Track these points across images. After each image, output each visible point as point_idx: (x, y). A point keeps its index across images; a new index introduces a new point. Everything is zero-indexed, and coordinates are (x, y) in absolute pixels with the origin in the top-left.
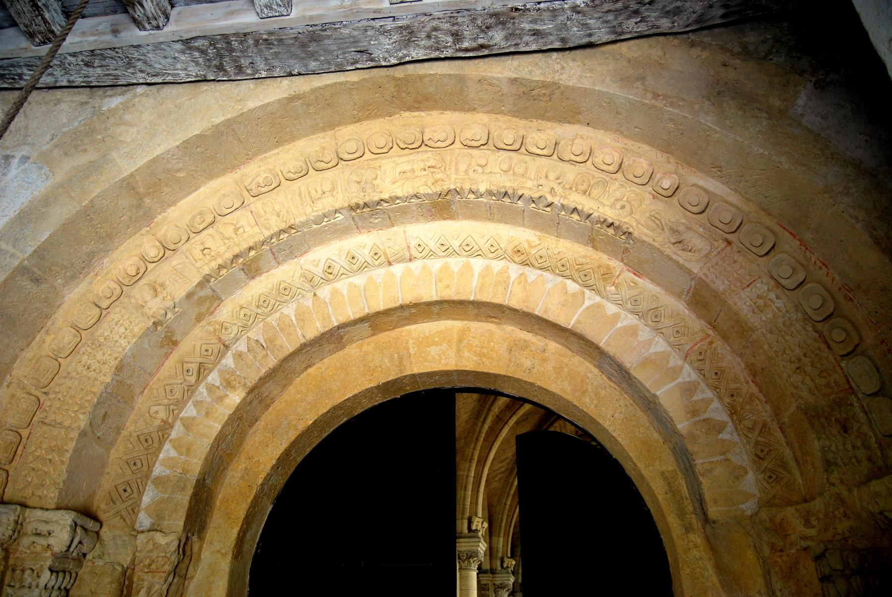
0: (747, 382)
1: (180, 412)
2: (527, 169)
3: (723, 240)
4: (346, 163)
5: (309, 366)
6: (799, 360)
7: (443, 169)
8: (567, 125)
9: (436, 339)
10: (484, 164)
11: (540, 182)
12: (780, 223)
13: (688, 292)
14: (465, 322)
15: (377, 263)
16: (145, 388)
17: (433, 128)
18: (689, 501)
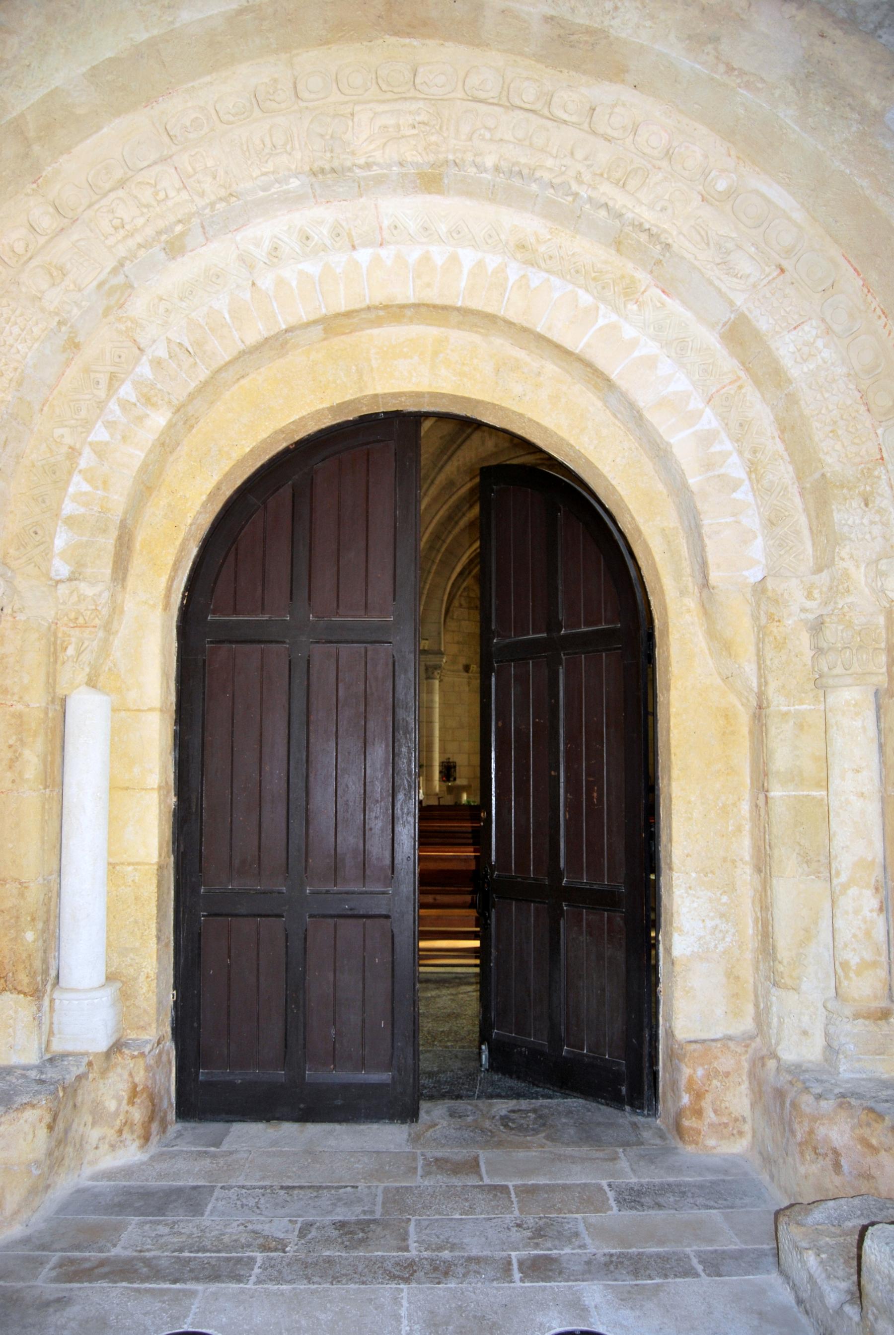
0: (773, 438)
1: (88, 436)
3: (776, 266)
5: (243, 377)
6: (835, 423)
7: (437, 127)
8: (607, 83)
9: (405, 350)
12: (846, 255)
13: (724, 325)
14: (442, 329)
16: (43, 405)
18: (688, 562)
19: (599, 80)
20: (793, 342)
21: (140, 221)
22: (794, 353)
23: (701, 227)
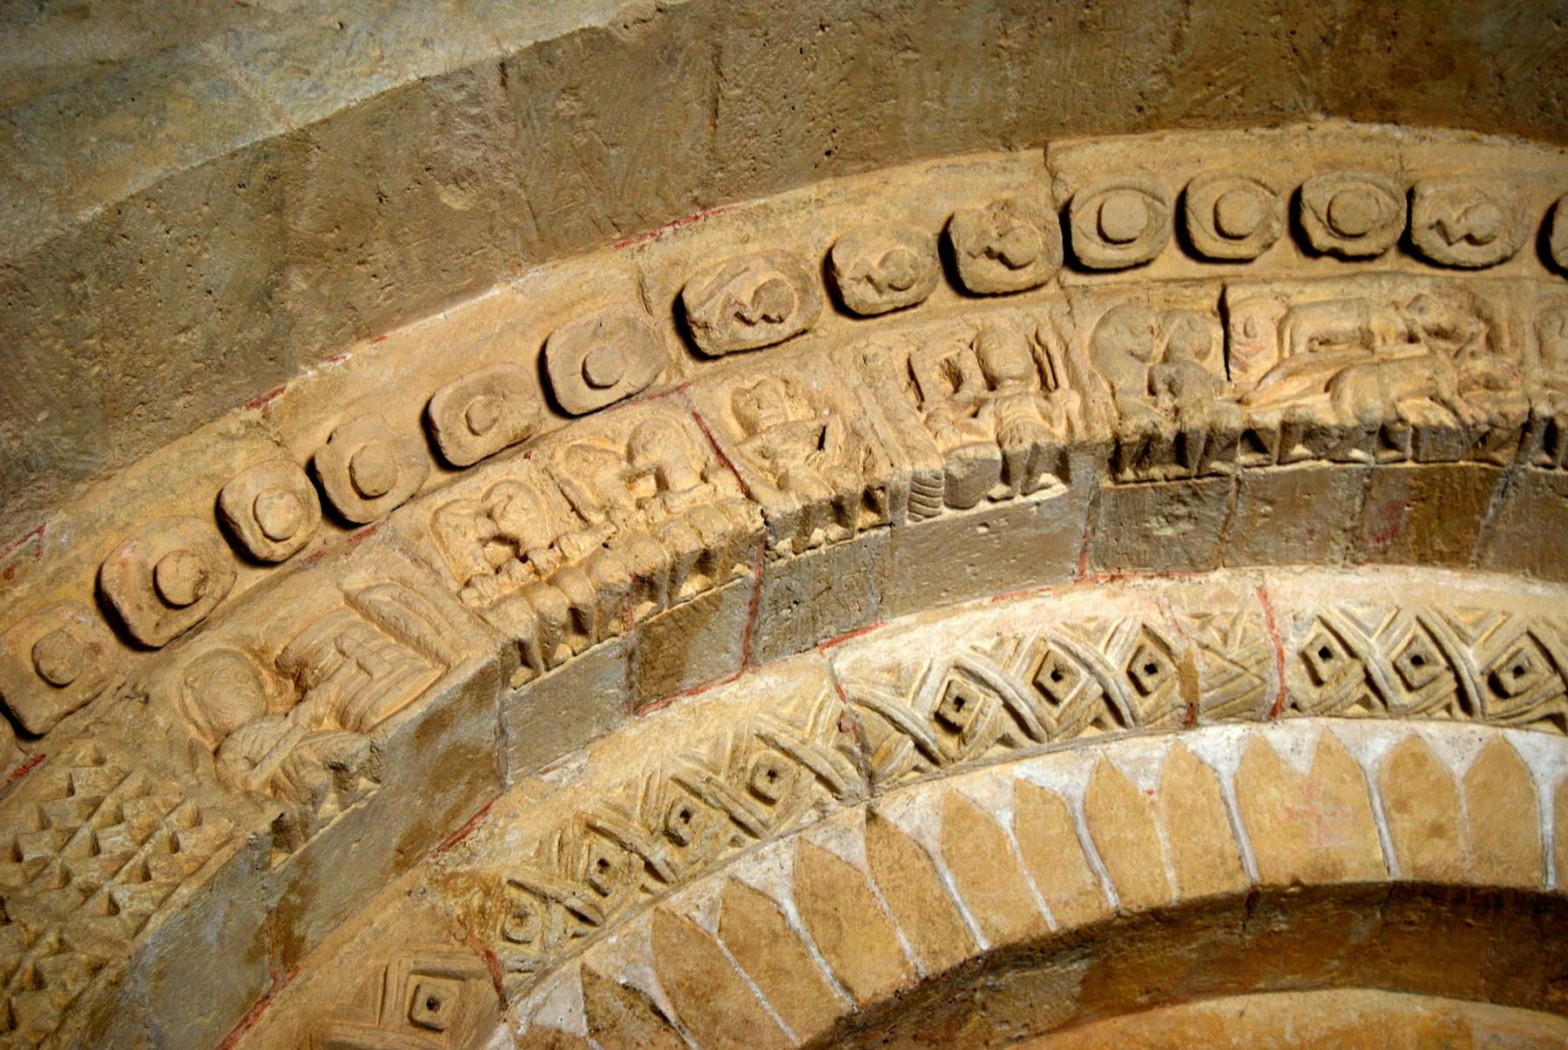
4: (1082, 280)
14: (1440, 1002)
15: (1143, 706)
17: (1450, 187)
21: (582, 545)
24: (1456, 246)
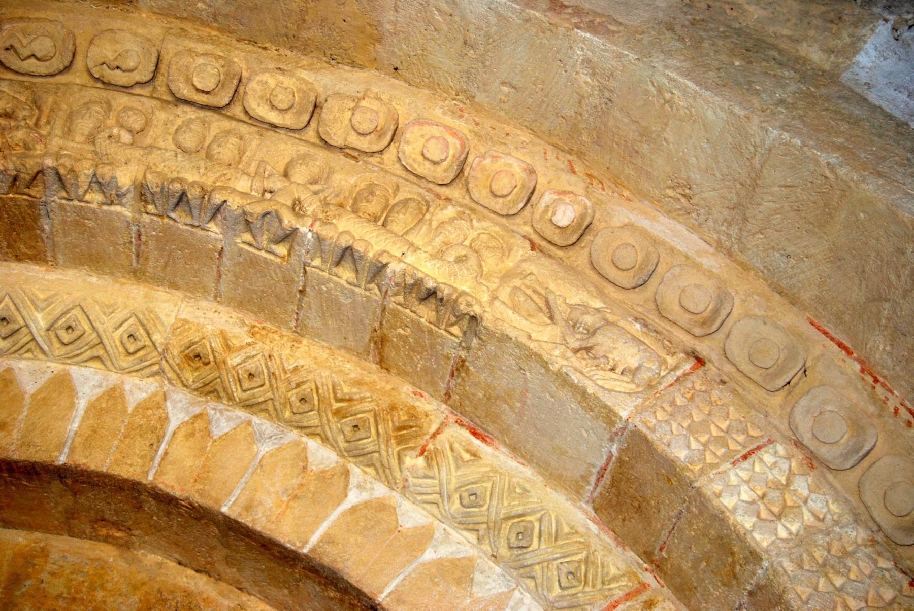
2: (242, 152)
3: (687, 354)
7: (31, 122)
10: (137, 126)
11: (269, 184)
12: (816, 321)
13: (601, 475)
14: (38, 535)
19: (333, 62)
20: (747, 482)
22: (753, 502)
23: (535, 291)
24: (28, 61)
